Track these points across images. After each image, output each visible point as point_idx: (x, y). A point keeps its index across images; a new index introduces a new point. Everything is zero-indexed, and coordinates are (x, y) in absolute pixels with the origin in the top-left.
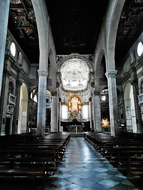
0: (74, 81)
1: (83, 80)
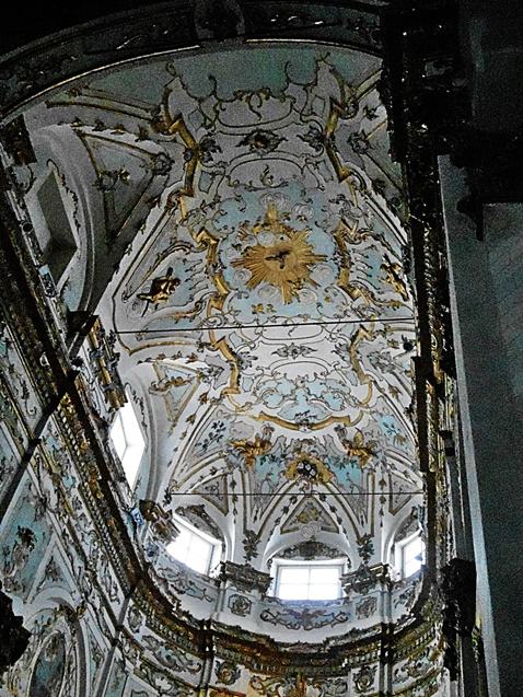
0: (310, 550)
1: (402, 533)
